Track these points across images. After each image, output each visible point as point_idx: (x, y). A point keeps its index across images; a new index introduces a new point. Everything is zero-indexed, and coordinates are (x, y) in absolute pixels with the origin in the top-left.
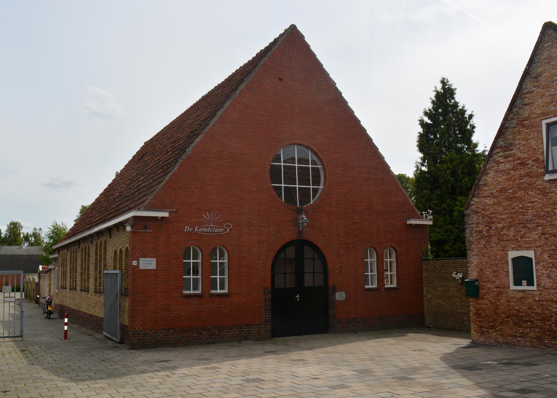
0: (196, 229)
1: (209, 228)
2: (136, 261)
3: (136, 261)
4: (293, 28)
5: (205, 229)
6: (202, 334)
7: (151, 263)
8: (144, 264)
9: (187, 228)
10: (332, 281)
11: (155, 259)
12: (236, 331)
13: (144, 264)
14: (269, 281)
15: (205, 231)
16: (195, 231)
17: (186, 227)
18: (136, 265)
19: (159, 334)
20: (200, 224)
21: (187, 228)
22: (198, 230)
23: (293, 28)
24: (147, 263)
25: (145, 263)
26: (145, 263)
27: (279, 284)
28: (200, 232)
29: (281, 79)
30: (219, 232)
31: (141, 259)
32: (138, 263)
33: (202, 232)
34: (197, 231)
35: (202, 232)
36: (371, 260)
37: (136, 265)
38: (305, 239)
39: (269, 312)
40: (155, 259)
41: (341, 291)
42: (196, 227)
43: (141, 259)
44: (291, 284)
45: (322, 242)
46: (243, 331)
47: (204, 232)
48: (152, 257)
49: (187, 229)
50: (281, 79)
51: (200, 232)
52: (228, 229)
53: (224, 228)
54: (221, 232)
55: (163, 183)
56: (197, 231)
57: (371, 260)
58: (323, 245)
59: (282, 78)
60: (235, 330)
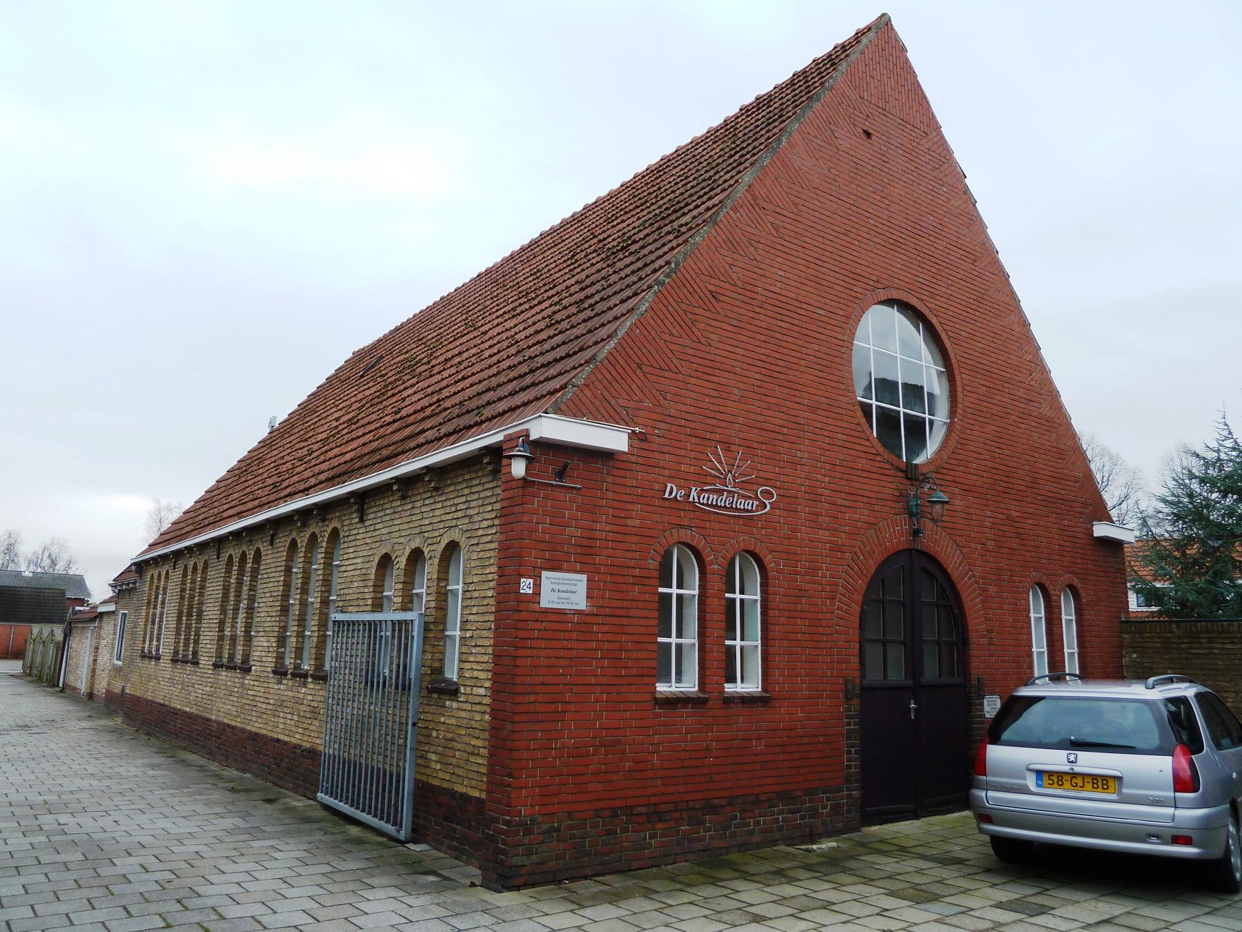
0: (693, 493)
1: (725, 493)
2: (531, 581)
3: (531, 581)
4: (883, 26)
5: (715, 496)
6: (702, 822)
7: (573, 588)
8: (553, 590)
9: (672, 489)
10: (977, 667)
11: (584, 577)
12: (781, 812)
13: (553, 590)
14: (855, 660)
15: (714, 503)
16: (691, 499)
17: (669, 485)
18: (531, 592)
19: (588, 829)
20: (702, 479)
21: (672, 489)
22: (699, 497)
23: (883, 26)
24: (562, 588)
25: (556, 587)
26: (556, 587)
27: (874, 676)
28: (703, 504)
29: (868, 135)
30: (748, 511)
31: (545, 574)
32: (537, 586)
33: (707, 505)
34: (696, 500)
35: (707, 505)
36: (1037, 613)
37: (531, 592)
38: (924, 550)
39: (856, 752)
40: (584, 577)
41: (992, 693)
42: (694, 489)
43: (545, 574)
44: (897, 675)
45: (956, 562)
46: (799, 811)
47: (711, 506)
48: (575, 572)
49: (673, 491)
50: (868, 135)
51: (703, 504)
52: (766, 502)
53: (758, 499)
54: (751, 511)
55: (612, 343)
56: (696, 500)
57: (1037, 613)
58: (957, 570)
59: (871, 131)
60: (781, 807)
